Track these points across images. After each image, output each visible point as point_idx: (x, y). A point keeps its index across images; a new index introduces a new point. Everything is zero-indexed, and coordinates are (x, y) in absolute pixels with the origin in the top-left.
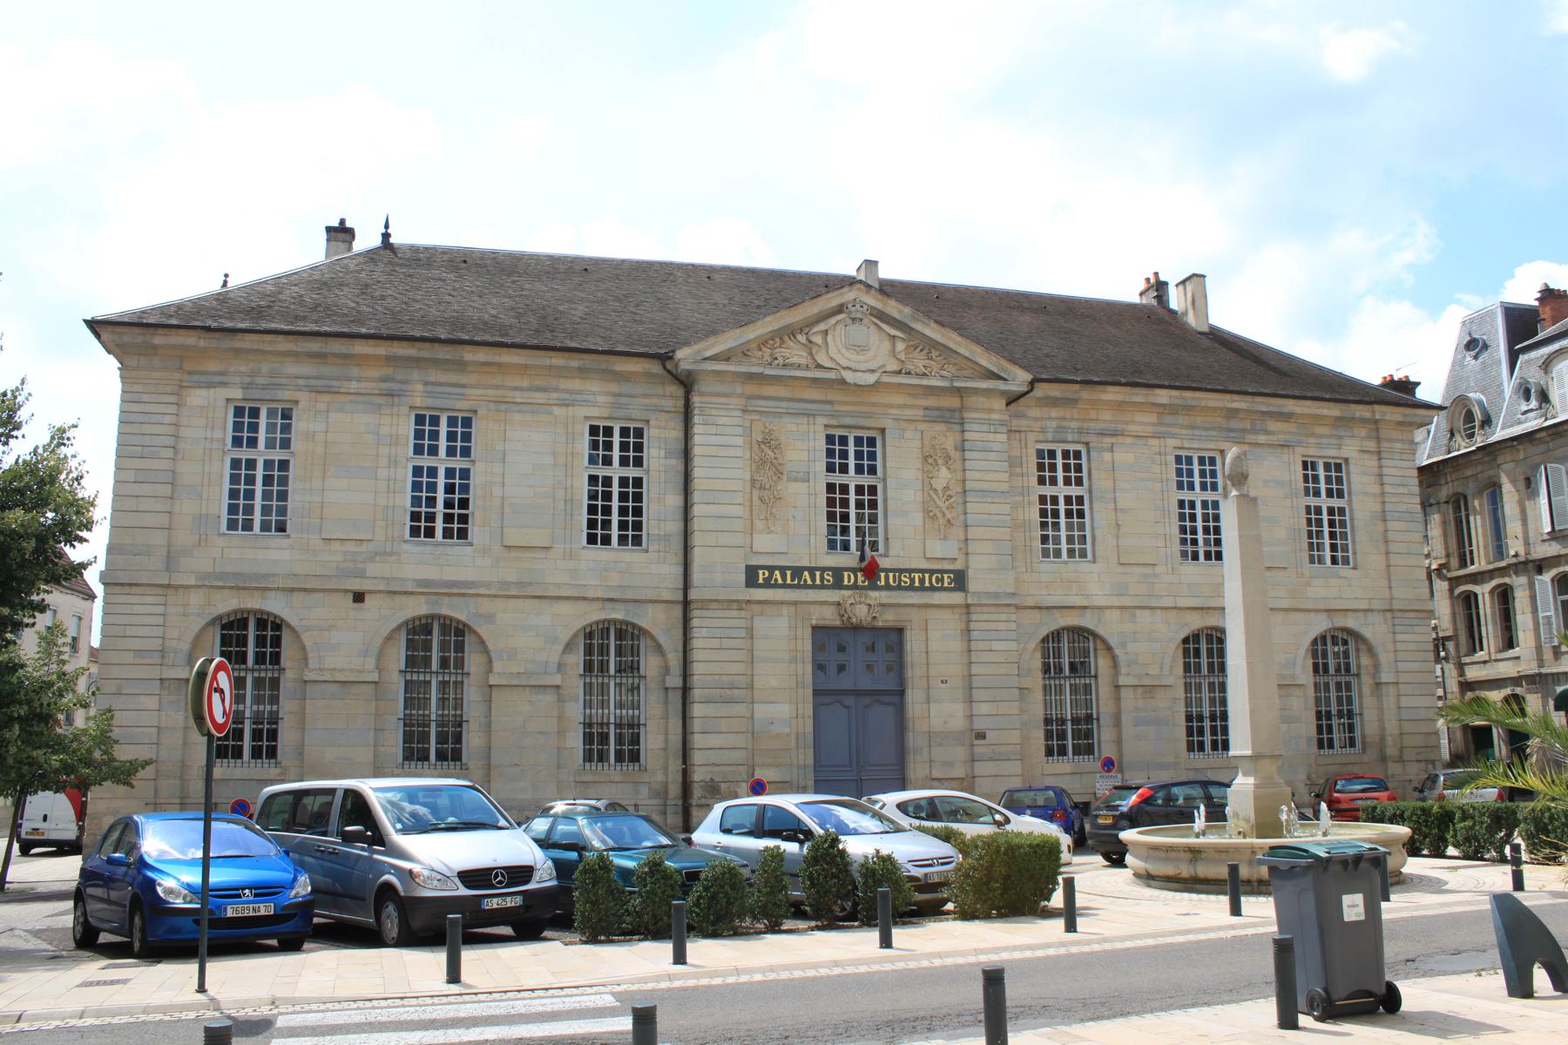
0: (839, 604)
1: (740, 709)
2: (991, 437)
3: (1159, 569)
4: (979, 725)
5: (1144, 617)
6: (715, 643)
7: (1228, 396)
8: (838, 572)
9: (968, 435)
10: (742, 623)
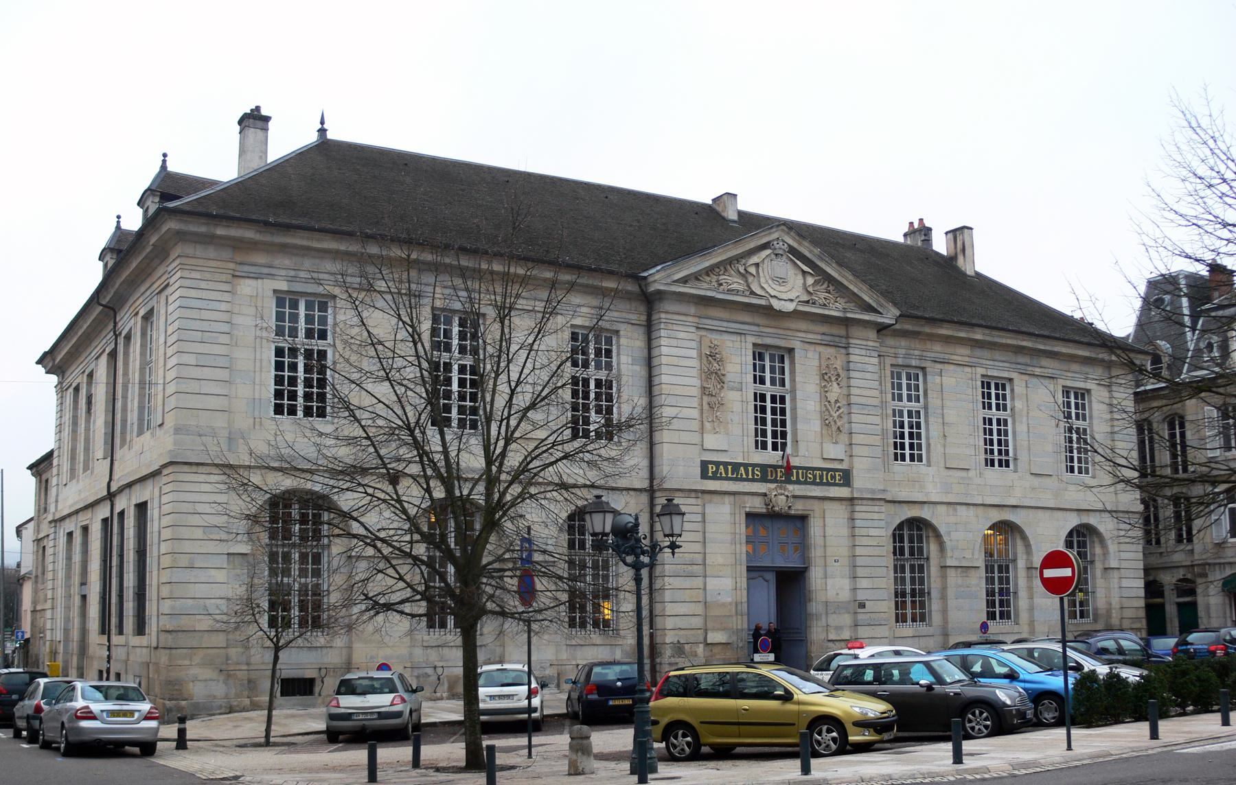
0: (765, 495)
1: (698, 582)
3: (972, 473)
4: (861, 596)
5: (962, 510)
7: (1020, 337)
8: (764, 468)
9: (852, 358)
10: (699, 509)
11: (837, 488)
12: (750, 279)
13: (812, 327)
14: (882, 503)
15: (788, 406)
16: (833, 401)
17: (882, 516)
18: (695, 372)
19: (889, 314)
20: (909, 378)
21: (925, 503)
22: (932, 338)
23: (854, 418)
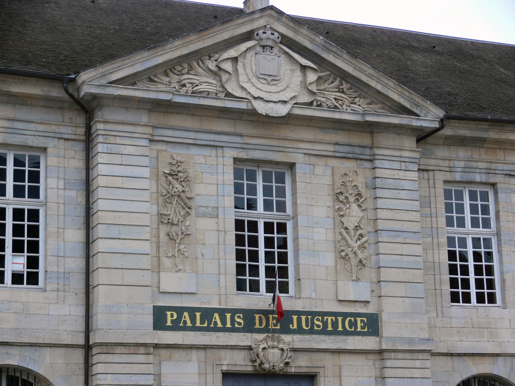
0: (250, 348)
2: (402, 174)
8: (248, 314)
9: (379, 173)
10: (150, 369)
11: (357, 338)
12: (225, 77)
13: (320, 135)
14: (427, 356)
15: (289, 235)
16: (351, 227)
17: (427, 373)
18: (146, 196)
19: (430, 116)
20: (473, 196)
21: (498, 355)
22: (502, 145)
23: (383, 248)
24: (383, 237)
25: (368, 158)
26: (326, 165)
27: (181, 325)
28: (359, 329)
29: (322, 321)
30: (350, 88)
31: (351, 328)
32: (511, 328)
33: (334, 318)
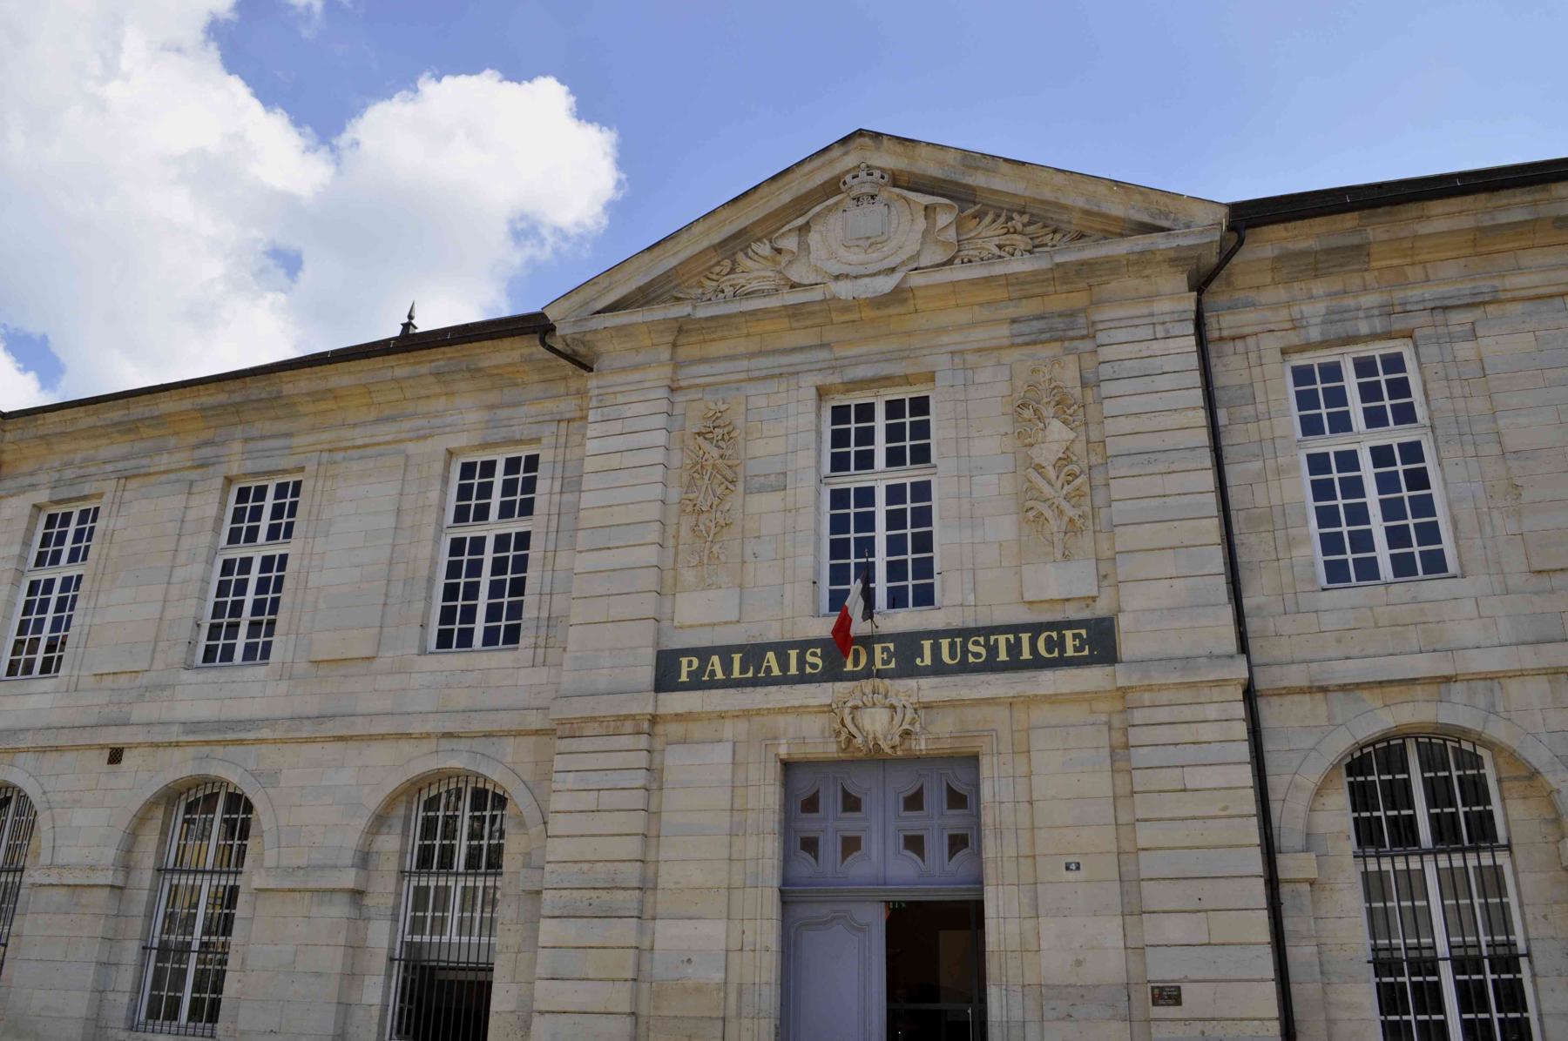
1: (624, 932)
2: (1156, 347)
4: (1162, 970)
6: (588, 801)
24: (1118, 468)
25: (1084, 332)
26: (999, 364)
27: (706, 678)
28: (1070, 652)
29: (986, 645)
30: (1030, 223)
31: (1050, 651)
32: (1480, 617)
33: (1011, 637)
